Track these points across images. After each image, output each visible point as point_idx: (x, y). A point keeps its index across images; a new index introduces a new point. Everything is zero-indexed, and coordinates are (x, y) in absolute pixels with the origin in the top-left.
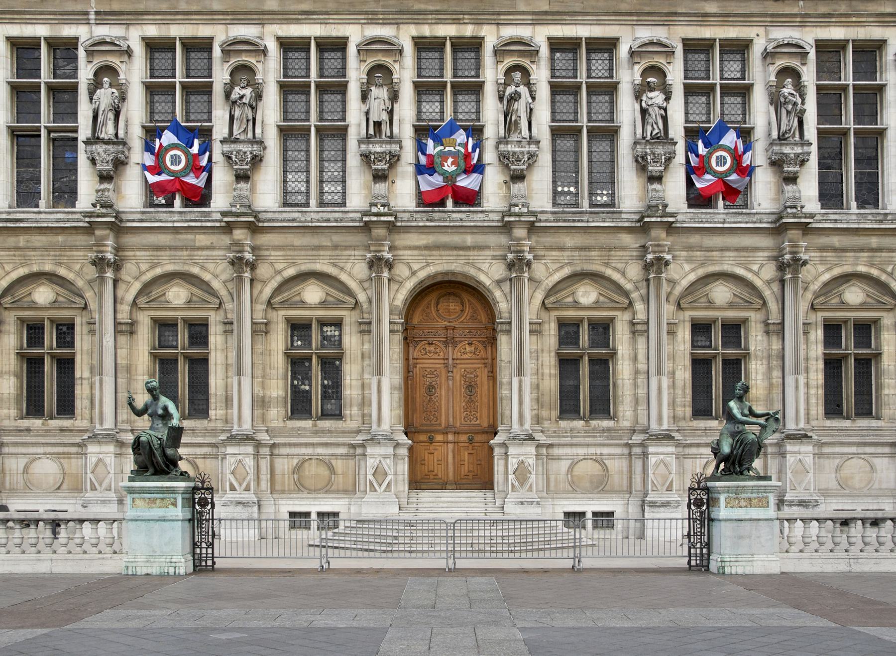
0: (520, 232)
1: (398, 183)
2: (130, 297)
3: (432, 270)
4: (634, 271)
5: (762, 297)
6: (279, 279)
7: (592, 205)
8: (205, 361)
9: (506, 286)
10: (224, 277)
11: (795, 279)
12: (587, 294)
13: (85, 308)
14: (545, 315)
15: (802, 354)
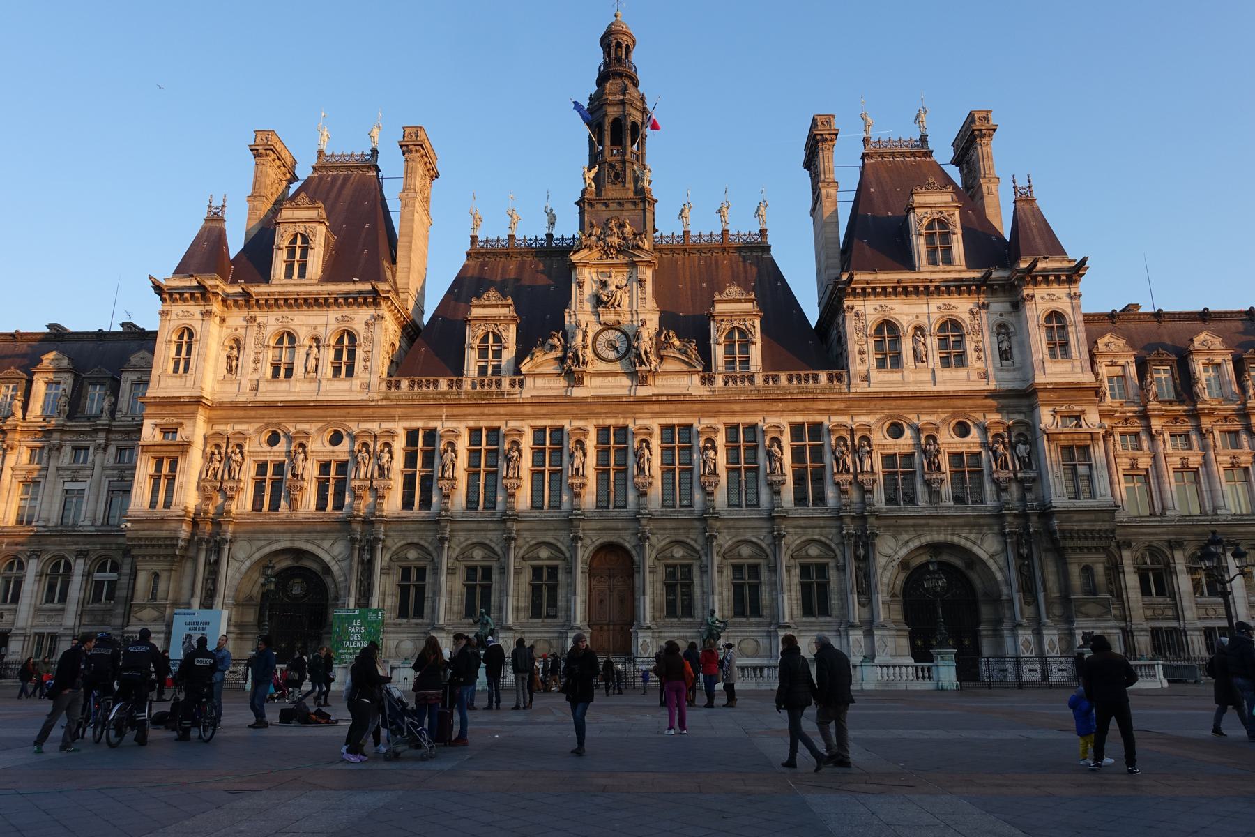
0: (644, 522)
1: (586, 497)
2: (454, 555)
3: (602, 540)
4: (701, 540)
5: (764, 551)
6: (528, 546)
7: (681, 506)
8: (490, 587)
9: (638, 549)
10: (501, 545)
11: (780, 545)
12: (678, 552)
13: (433, 560)
14: (657, 563)
15: (785, 582)
